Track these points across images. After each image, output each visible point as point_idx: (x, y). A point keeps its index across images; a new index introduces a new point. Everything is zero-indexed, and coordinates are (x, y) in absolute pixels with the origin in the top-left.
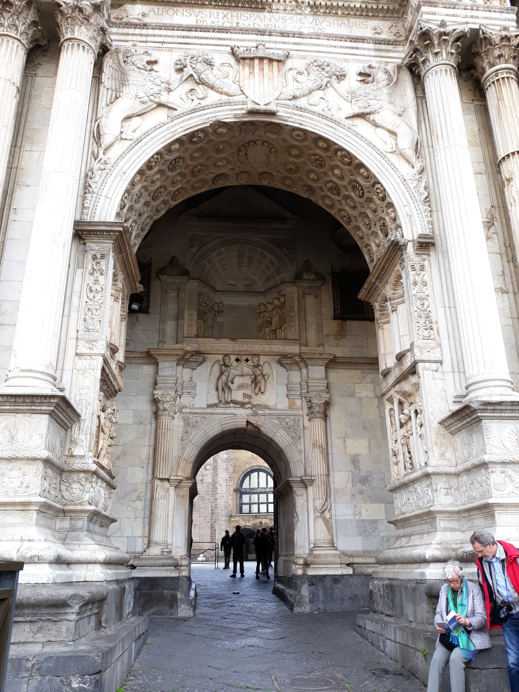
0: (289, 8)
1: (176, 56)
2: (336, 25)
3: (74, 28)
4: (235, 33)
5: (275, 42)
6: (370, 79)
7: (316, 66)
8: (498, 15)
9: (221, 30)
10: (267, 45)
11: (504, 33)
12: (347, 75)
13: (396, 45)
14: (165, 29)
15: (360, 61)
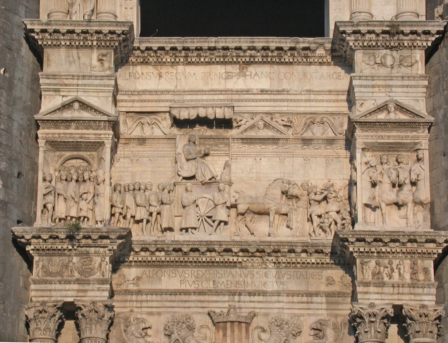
0: (256, 265)
1: (163, 319)
2: (295, 278)
3: (92, 327)
4: (212, 295)
5: (244, 302)
6: (321, 334)
7: (277, 326)
8: (420, 291)
9: (201, 293)
10: (237, 305)
11: (422, 311)
12: (303, 332)
13: (345, 297)
14: (156, 295)
15: (313, 315)
